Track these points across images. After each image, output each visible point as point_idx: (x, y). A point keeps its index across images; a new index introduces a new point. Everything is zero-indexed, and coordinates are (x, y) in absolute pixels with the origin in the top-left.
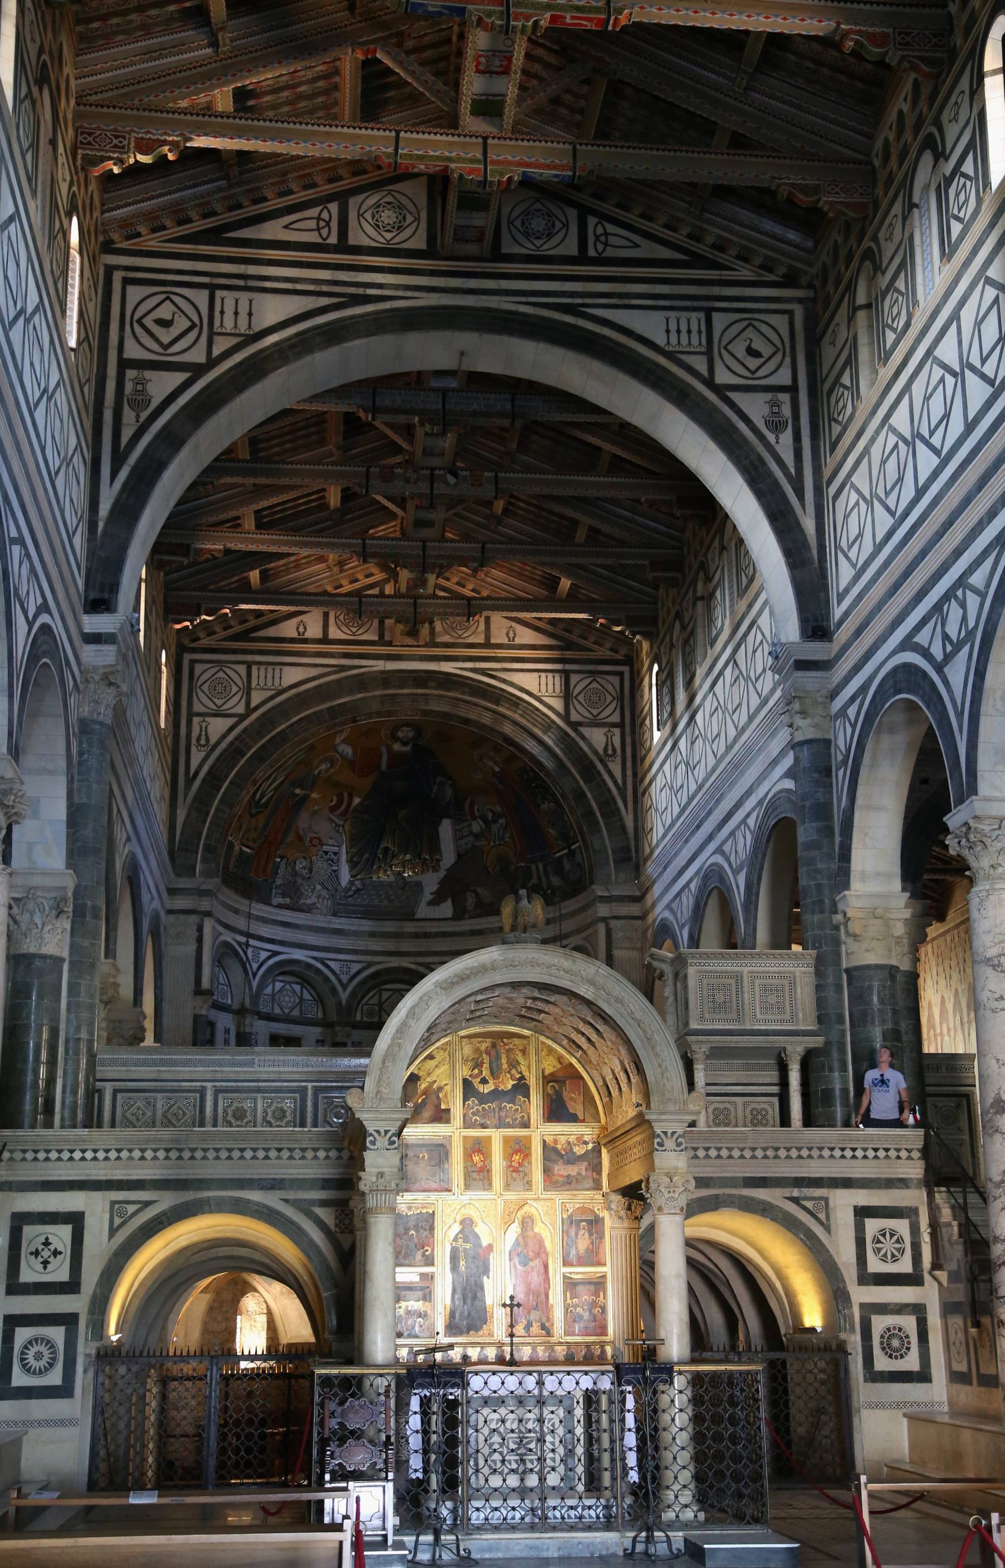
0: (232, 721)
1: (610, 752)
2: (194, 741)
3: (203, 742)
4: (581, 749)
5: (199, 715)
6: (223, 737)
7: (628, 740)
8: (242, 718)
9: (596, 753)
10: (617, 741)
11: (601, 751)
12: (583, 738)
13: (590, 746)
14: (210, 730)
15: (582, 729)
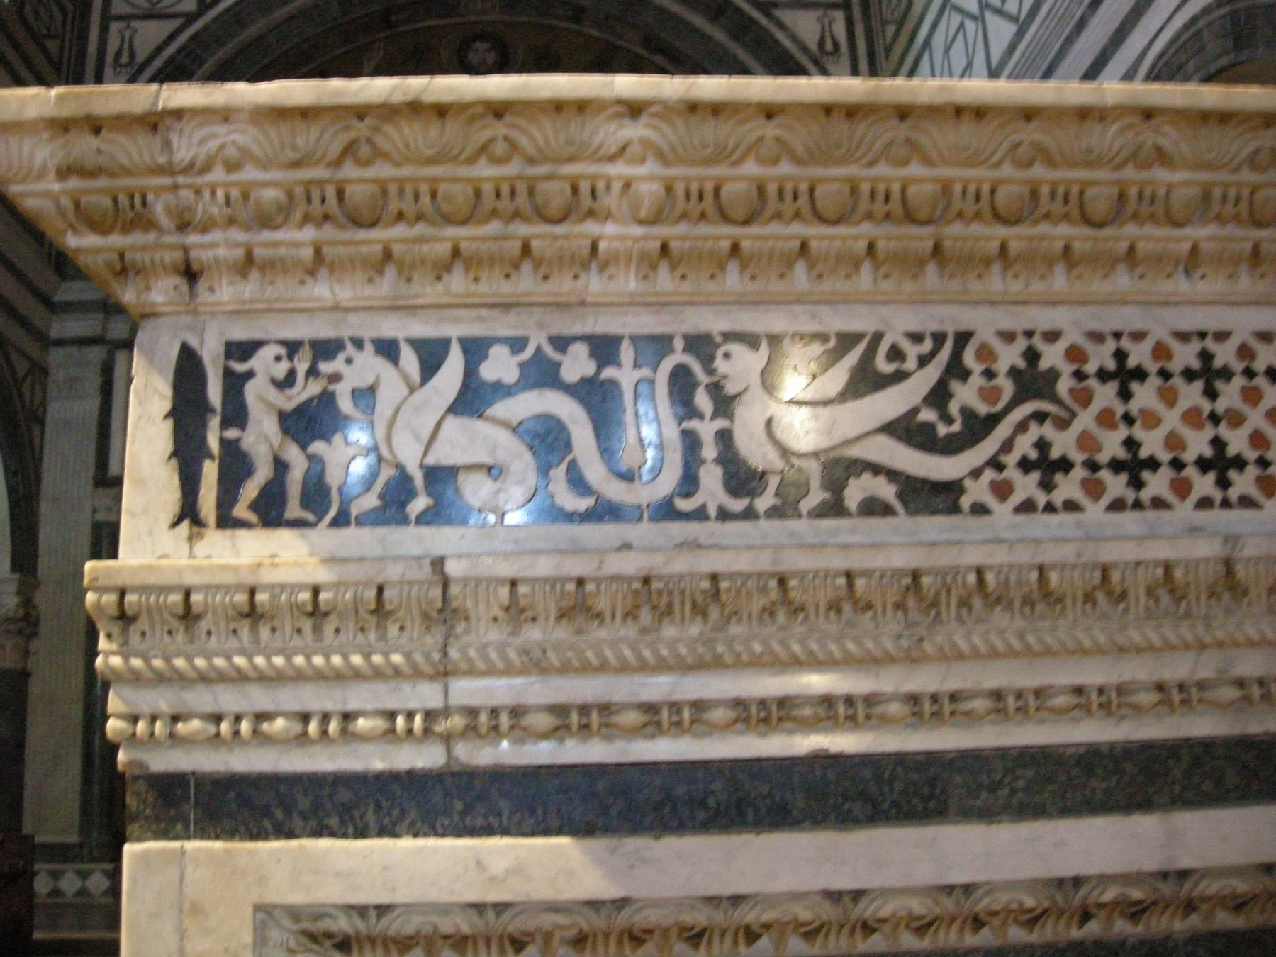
0: (173, 25)
1: (829, 46)
2: (109, 59)
3: (125, 59)
4: (777, 42)
5: (120, 18)
6: (159, 50)
7: (859, 29)
8: (190, 18)
9: (804, 49)
10: (840, 30)
11: (813, 45)
12: (781, 26)
13: (794, 38)
14: (136, 43)
15: (778, 13)
